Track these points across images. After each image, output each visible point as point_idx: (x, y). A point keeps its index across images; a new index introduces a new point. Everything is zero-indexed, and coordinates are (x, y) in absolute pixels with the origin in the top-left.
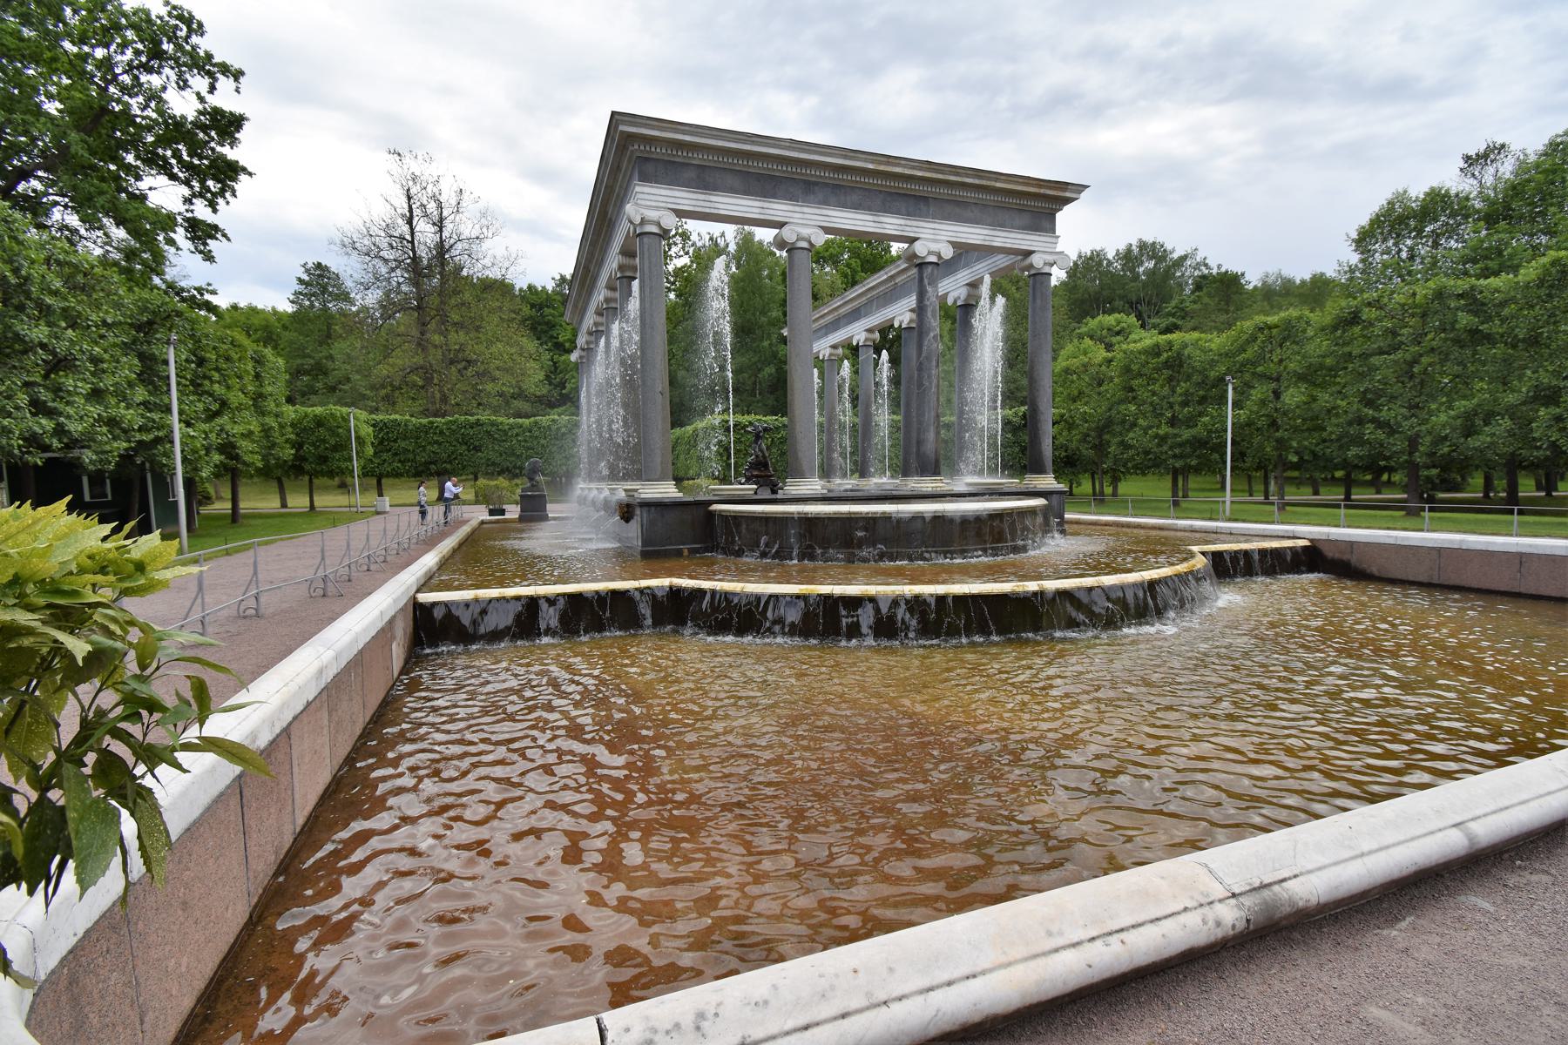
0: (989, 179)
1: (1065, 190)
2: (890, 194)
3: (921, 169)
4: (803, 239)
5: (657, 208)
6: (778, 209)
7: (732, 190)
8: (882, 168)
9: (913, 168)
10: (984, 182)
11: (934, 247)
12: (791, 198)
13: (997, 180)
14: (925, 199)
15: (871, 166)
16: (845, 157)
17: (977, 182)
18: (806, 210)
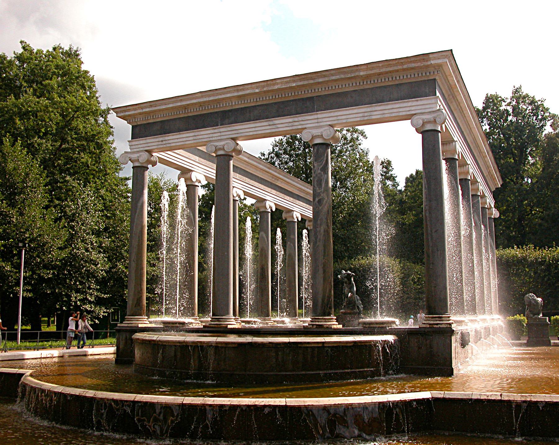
0: (352, 72)
1: (429, 60)
2: (283, 103)
3: (294, 81)
4: (220, 149)
5: (138, 152)
6: (205, 133)
7: (180, 130)
8: (265, 89)
9: (287, 82)
10: (349, 76)
11: (316, 132)
12: (214, 124)
13: (359, 71)
14: (311, 99)
15: (257, 91)
16: (238, 91)
17: (343, 76)
18: (222, 130)
